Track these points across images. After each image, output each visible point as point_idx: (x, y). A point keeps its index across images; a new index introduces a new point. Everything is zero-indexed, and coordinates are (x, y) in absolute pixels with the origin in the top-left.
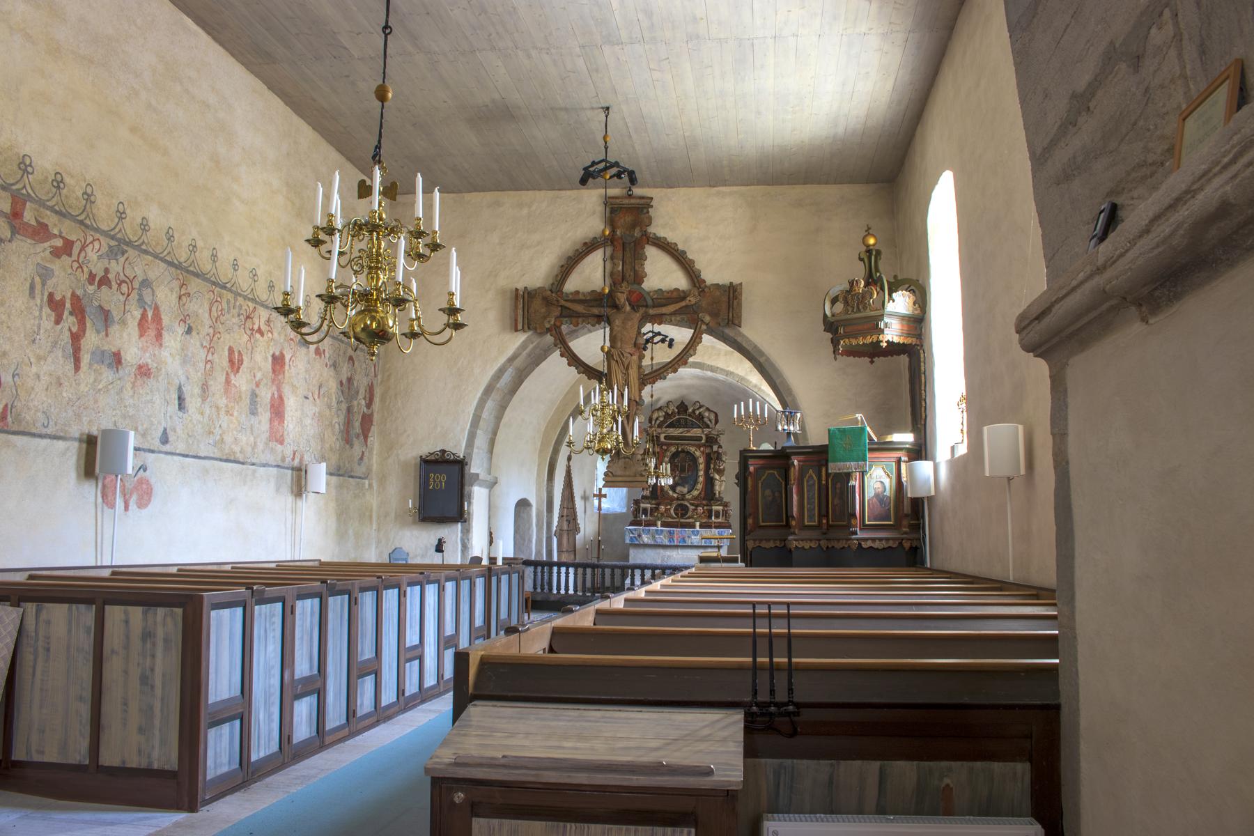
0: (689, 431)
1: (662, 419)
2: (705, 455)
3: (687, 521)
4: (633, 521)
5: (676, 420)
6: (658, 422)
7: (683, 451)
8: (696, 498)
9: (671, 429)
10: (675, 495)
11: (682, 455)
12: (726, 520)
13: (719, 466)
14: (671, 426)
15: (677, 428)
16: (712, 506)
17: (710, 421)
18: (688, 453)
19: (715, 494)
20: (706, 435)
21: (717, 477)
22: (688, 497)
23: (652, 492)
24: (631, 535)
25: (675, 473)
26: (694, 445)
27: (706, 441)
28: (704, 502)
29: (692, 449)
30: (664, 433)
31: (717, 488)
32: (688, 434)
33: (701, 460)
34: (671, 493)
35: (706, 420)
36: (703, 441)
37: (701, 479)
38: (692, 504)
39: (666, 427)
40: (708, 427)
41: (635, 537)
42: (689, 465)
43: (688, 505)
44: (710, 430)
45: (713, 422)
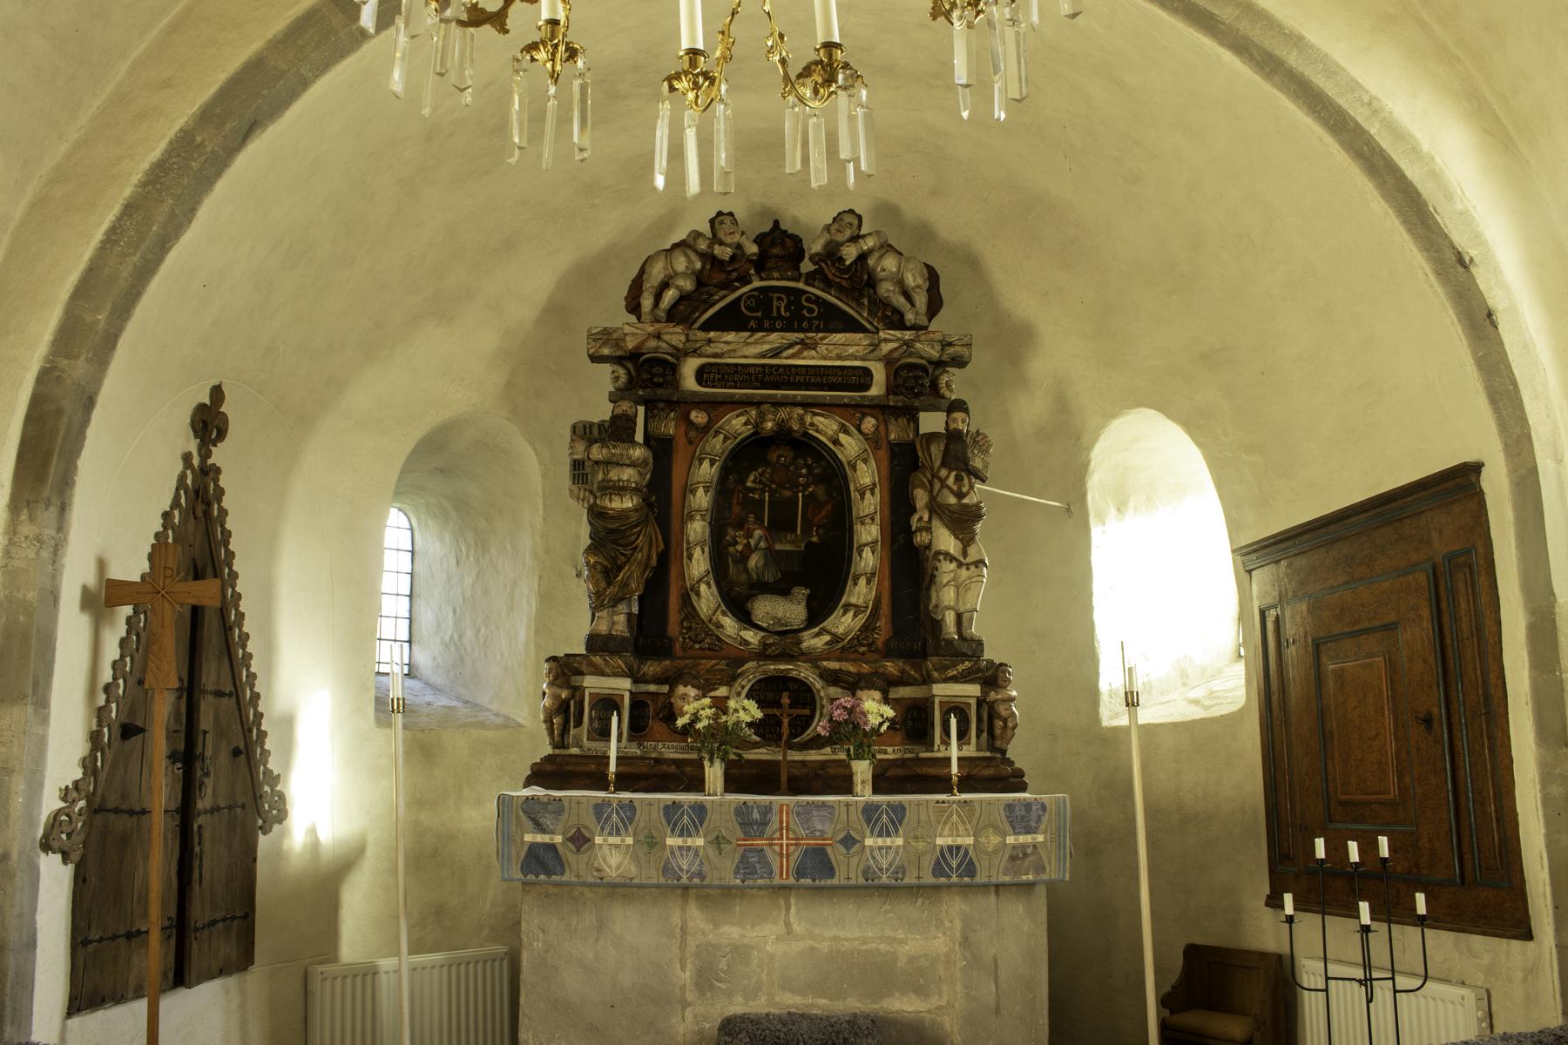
0: (813, 347)
1: (688, 285)
2: (883, 453)
3: (813, 756)
4: (548, 759)
5: (749, 296)
6: (670, 295)
7: (784, 436)
8: (843, 648)
9: (731, 336)
10: (752, 637)
11: (780, 455)
12: (992, 747)
13: (960, 495)
14: (730, 320)
15: (754, 331)
16: (927, 681)
19: (937, 625)
20: (888, 361)
22: (814, 641)
23: (639, 623)
25: (749, 535)
26: (829, 407)
27: (892, 389)
28: (891, 667)
29: (825, 426)
30: (695, 352)
31: (948, 596)
32: (809, 360)
33: (865, 475)
34: (729, 624)
35: (886, 289)
36: (877, 390)
37: (868, 560)
38: (832, 678)
39: (706, 327)
40: (896, 320)
41: (552, 847)
42: (810, 499)
43: (818, 684)
44: (908, 335)
45: (921, 300)
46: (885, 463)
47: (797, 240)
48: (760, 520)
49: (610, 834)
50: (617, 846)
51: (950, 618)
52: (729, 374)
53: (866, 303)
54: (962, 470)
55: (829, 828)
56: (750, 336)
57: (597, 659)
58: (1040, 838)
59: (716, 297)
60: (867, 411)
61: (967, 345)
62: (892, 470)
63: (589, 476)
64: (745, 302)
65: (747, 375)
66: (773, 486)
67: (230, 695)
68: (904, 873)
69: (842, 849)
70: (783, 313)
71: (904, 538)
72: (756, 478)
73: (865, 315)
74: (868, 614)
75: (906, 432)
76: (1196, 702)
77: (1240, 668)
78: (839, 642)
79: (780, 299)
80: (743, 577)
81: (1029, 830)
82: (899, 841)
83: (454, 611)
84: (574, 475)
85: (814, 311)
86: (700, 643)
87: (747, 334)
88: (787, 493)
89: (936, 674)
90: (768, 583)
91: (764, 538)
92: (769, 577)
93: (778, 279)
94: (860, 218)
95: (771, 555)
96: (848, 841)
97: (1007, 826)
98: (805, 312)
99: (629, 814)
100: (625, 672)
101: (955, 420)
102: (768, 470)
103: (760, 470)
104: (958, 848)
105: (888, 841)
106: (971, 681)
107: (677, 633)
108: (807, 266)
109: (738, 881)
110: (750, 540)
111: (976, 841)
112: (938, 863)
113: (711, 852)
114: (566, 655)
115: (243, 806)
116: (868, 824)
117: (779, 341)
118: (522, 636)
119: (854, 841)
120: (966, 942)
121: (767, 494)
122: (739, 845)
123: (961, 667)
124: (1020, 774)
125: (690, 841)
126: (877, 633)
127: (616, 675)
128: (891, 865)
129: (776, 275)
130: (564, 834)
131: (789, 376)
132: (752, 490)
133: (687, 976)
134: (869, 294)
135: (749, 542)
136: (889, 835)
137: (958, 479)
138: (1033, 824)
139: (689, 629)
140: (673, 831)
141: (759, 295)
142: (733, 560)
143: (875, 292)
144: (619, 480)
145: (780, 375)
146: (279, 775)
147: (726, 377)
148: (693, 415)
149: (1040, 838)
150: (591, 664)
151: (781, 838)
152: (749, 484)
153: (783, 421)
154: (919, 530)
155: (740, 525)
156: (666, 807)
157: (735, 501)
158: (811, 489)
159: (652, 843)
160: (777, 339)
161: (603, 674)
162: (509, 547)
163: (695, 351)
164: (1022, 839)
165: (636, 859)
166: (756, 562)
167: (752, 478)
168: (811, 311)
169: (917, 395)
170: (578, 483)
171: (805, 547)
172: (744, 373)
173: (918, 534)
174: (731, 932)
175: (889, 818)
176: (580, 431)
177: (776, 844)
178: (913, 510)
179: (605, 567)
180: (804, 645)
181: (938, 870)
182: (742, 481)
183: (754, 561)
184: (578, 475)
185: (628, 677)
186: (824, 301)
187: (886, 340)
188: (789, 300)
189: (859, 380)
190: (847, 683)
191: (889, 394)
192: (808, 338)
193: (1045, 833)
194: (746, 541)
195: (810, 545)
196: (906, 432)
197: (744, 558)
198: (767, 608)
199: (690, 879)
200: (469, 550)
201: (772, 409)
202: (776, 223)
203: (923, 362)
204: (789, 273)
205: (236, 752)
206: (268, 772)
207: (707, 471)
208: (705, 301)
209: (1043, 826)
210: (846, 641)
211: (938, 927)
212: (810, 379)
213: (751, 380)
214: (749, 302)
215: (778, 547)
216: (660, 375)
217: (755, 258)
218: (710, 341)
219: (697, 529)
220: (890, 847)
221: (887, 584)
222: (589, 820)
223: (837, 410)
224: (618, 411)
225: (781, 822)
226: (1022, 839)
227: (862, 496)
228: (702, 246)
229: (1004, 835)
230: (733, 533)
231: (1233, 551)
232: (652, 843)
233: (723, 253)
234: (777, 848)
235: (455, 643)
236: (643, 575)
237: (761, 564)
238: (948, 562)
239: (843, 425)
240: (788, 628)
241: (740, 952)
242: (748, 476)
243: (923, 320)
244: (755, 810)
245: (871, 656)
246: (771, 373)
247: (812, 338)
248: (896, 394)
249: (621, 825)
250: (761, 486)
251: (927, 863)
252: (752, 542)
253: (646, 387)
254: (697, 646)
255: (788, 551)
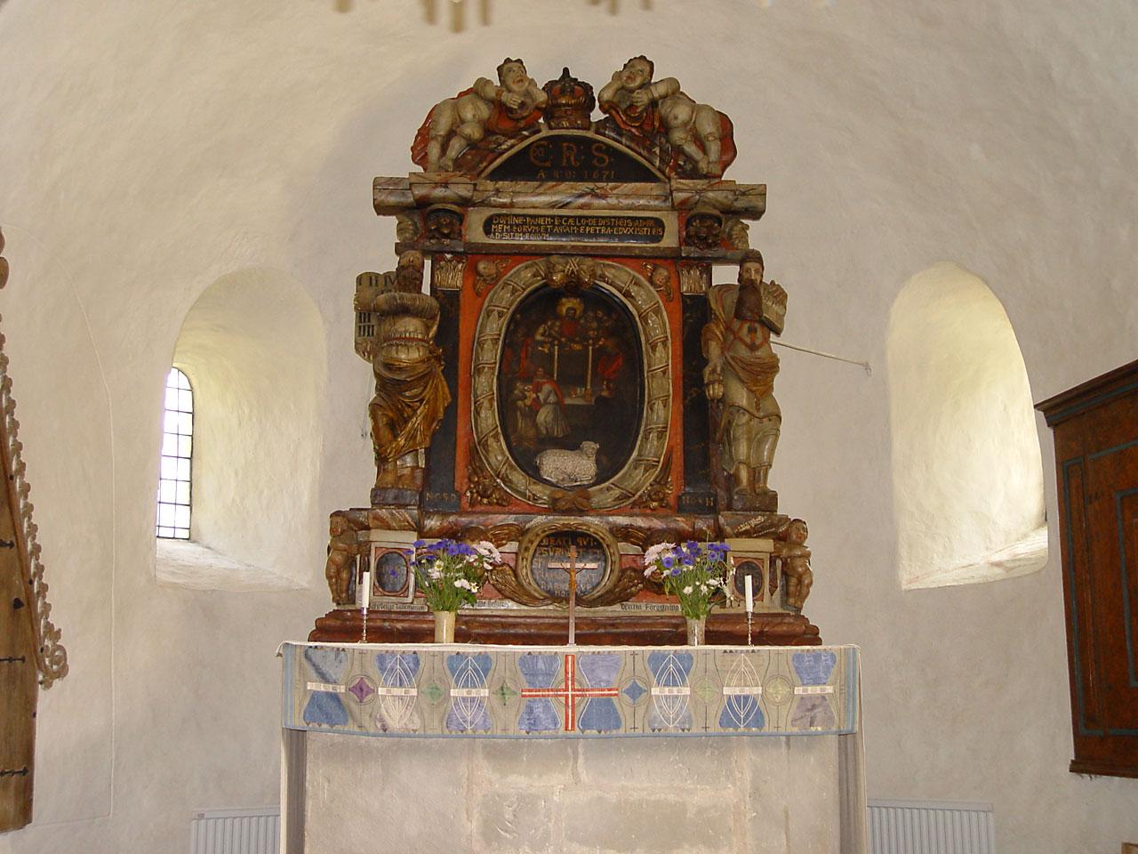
2: (677, 306)
6: (456, 147)
7: (573, 287)
10: (538, 489)
12: (784, 603)
13: (753, 347)
14: (520, 168)
17: (700, 143)
18: (598, 301)
21: (741, 396)
22: (605, 495)
24: (315, 686)
25: (538, 389)
27: (686, 240)
29: (617, 279)
30: (484, 203)
34: (518, 478)
36: (670, 240)
41: (334, 697)
44: (700, 184)
45: (714, 148)
46: (678, 316)
47: (587, 88)
48: (549, 374)
49: (394, 685)
50: (401, 698)
51: (744, 474)
52: (517, 225)
53: (658, 152)
54: (756, 321)
55: (615, 679)
56: (539, 186)
57: (383, 513)
58: (829, 689)
59: (504, 147)
60: (658, 262)
61: (761, 195)
62: (684, 323)
63: (375, 328)
64: (534, 152)
65: (535, 226)
66: (563, 339)
67: (11, 545)
68: (691, 723)
69: (626, 698)
70: (573, 163)
71: (695, 391)
72: (545, 331)
73: (657, 163)
74: (659, 469)
75: (699, 283)
76: (998, 565)
77: (1044, 533)
78: (630, 497)
79: (568, 148)
80: (532, 432)
81: (816, 682)
82: (686, 691)
83: (236, 474)
84: (360, 327)
85: (605, 161)
86: (488, 498)
87: (536, 184)
88: (577, 347)
89: (728, 529)
90: (557, 438)
91: (553, 392)
92: (558, 432)
93: (567, 128)
94: (651, 64)
95: (562, 410)
96: (635, 692)
97: (795, 676)
98: (595, 162)
99: (412, 665)
100: (412, 526)
101: (748, 270)
102: (558, 324)
103: (549, 323)
104: (746, 698)
105: (675, 691)
106: (765, 536)
107: (465, 488)
108: (597, 115)
109: (523, 732)
110: (539, 394)
111: (764, 691)
112: (725, 713)
113: (496, 702)
114: (351, 509)
115: (23, 659)
116: (655, 673)
117: (569, 191)
118: (305, 499)
119: (641, 691)
120: (756, 793)
121: (556, 347)
122: (525, 696)
123: (753, 522)
124: (815, 631)
125: (474, 693)
126: (668, 489)
127: (402, 529)
128: (677, 716)
129: (565, 124)
130: (346, 684)
131: (579, 227)
132: (542, 344)
133: (473, 826)
134: (661, 143)
135: (538, 397)
136: (675, 684)
137: (752, 331)
138: (822, 675)
139: (478, 483)
140: (457, 682)
141: (548, 144)
142: (521, 414)
143: (668, 141)
144: (406, 331)
145: (570, 226)
146: (60, 630)
147: (515, 228)
148: (481, 266)
149: (829, 689)
150: (376, 518)
151: (567, 690)
152: (539, 338)
153: (573, 272)
154: (713, 383)
155: (528, 379)
156: (451, 658)
157: (523, 355)
158: (601, 343)
159: (437, 694)
160: (567, 190)
161: (389, 528)
162: (292, 407)
163: (482, 202)
164: (811, 690)
165: (419, 710)
166: (546, 417)
167: (541, 330)
168: (601, 161)
169: (709, 246)
170: (364, 335)
171: (595, 401)
172: (533, 224)
173: (711, 386)
174: (518, 782)
175: (676, 667)
176: (366, 282)
177: (561, 696)
178: (706, 362)
179: (392, 419)
180: (595, 500)
181: (726, 721)
182: (530, 334)
183: (544, 416)
184: (364, 327)
185: (415, 531)
186: (616, 151)
187: (679, 190)
188: (578, 148)
189: (651, 232)
190: (638, 538)
191: (681, 245)
192: (598, 188)
193: (833, 684)
194: (534, 395)
195: (600, 400)
196: (699, 283)
197: (533, 411)
198: (556, 464)
199: (474, 731)
200: (251, 410)
201: (561, 260)
202: (566, 71)
203: (716, 212)
204: (579, 122)
205: (17, 604)
206: (49, 627)
207: (495, 327)
208: (493, 151)
209: (831, 678)
210: (637, 496)
211: (727, 777)
212: (600, 230)
213: (540, 231)
214: (538, 152)
215: (568, 401)
216: (447, 226)
217: (544, 106)
218: (498, 191)
219: (486, 384)
220: (677, 697)
221: (679, 439)
222: (373, 670)
223: (630, 262)
224: (404, 262)
225: (567, 673)
226: (811, 690)
227: (654, 348)
228: (491, 94)
229: (793, 687)
230: (521, 387)
231: (1035, 406)
232: (437, 694)
233: (512, 100)
234: (563, 699)
235: (237, 505)
236: (430, 428)
237: (549, 419)
238: (741, 415)
239: (634, 277)
240: (578, 483)
241: (527, 803)
242: (538, 328)
243: (716, 170)
244: (540, 661)
245: (662, 512)
246: (561, 224)
247: (602, 188)
248: (688, 244)
249: (404, 677)
250: (550, 340)
251: (715, 711)
252: (542, 397)
253: (433, 237)
254: (485, 501)
255: (579, 406)
